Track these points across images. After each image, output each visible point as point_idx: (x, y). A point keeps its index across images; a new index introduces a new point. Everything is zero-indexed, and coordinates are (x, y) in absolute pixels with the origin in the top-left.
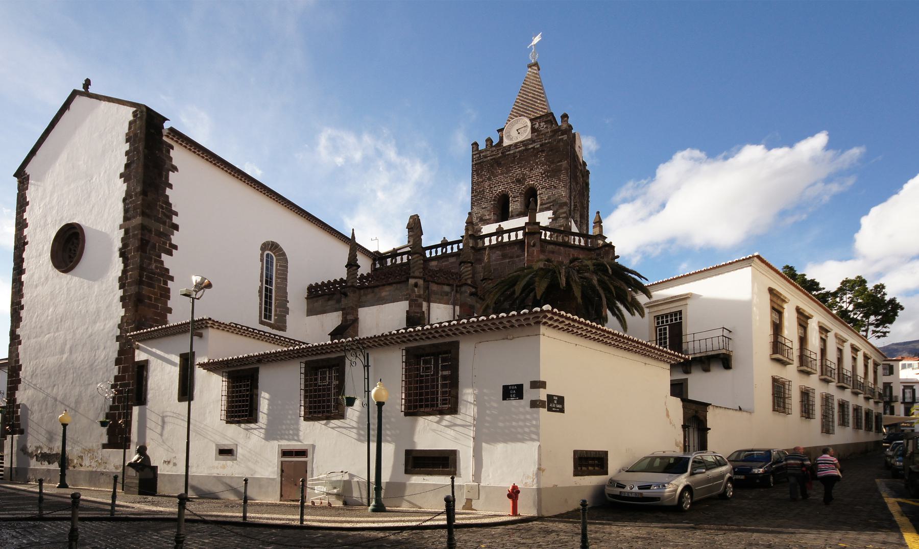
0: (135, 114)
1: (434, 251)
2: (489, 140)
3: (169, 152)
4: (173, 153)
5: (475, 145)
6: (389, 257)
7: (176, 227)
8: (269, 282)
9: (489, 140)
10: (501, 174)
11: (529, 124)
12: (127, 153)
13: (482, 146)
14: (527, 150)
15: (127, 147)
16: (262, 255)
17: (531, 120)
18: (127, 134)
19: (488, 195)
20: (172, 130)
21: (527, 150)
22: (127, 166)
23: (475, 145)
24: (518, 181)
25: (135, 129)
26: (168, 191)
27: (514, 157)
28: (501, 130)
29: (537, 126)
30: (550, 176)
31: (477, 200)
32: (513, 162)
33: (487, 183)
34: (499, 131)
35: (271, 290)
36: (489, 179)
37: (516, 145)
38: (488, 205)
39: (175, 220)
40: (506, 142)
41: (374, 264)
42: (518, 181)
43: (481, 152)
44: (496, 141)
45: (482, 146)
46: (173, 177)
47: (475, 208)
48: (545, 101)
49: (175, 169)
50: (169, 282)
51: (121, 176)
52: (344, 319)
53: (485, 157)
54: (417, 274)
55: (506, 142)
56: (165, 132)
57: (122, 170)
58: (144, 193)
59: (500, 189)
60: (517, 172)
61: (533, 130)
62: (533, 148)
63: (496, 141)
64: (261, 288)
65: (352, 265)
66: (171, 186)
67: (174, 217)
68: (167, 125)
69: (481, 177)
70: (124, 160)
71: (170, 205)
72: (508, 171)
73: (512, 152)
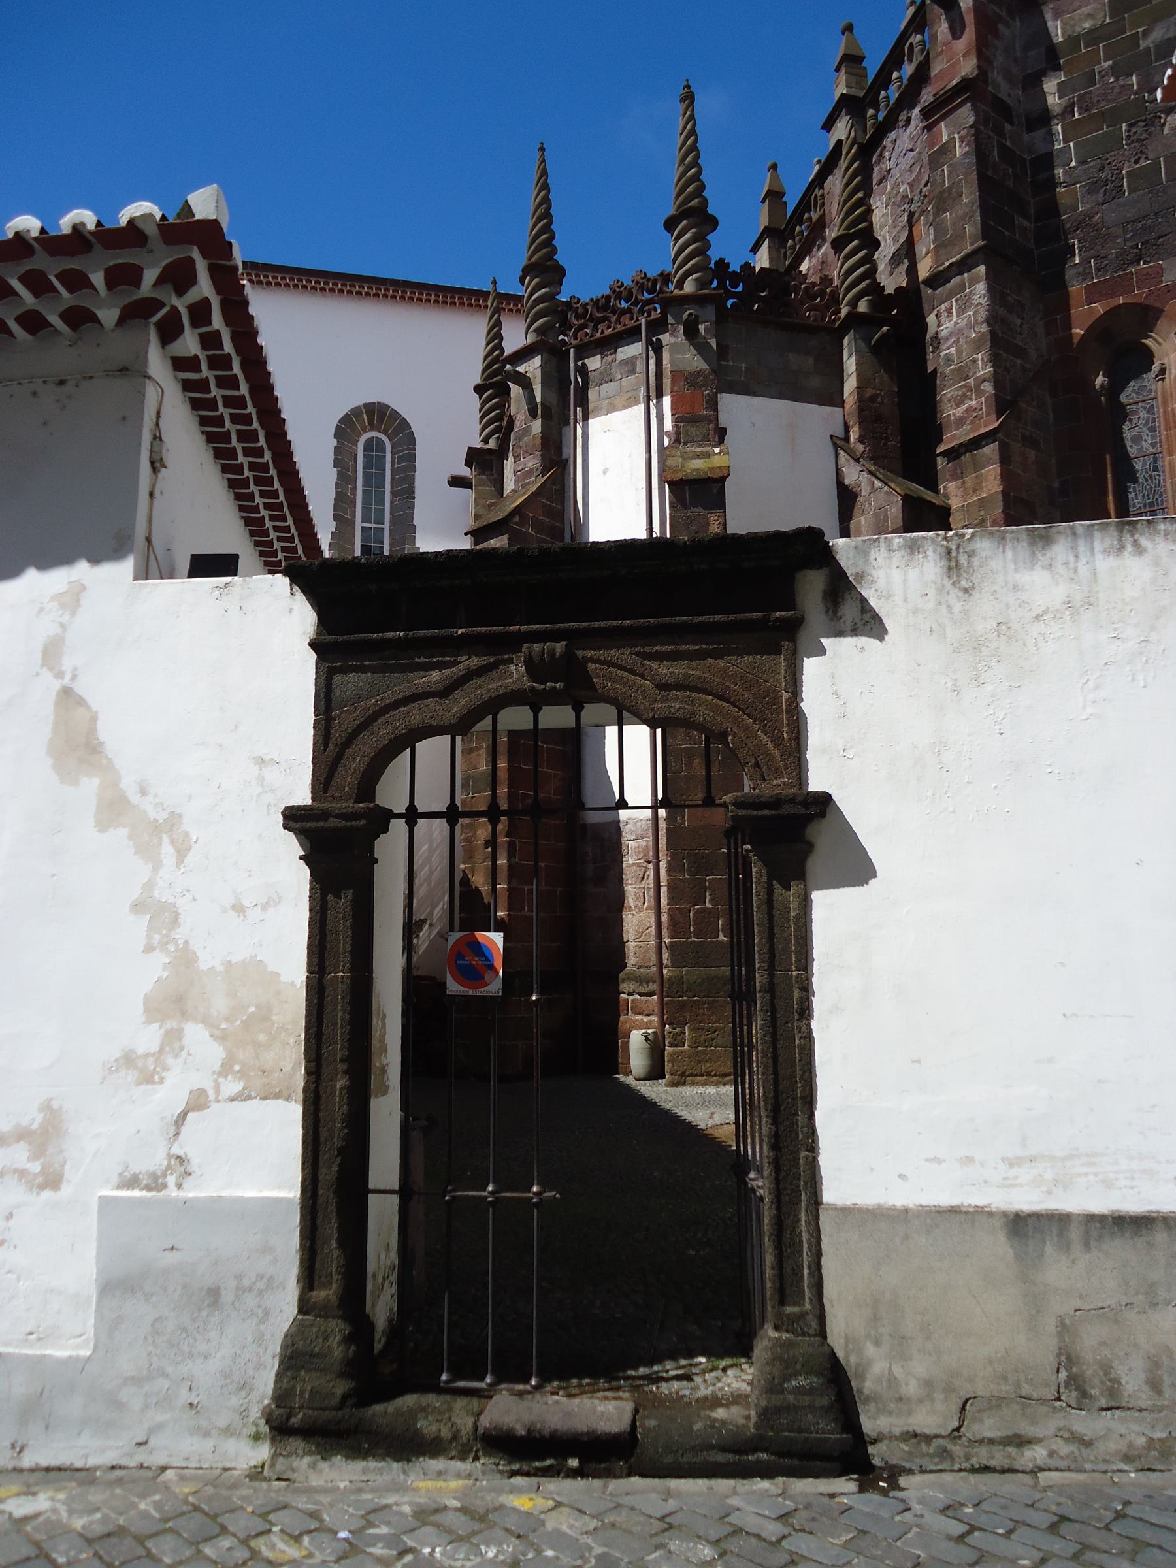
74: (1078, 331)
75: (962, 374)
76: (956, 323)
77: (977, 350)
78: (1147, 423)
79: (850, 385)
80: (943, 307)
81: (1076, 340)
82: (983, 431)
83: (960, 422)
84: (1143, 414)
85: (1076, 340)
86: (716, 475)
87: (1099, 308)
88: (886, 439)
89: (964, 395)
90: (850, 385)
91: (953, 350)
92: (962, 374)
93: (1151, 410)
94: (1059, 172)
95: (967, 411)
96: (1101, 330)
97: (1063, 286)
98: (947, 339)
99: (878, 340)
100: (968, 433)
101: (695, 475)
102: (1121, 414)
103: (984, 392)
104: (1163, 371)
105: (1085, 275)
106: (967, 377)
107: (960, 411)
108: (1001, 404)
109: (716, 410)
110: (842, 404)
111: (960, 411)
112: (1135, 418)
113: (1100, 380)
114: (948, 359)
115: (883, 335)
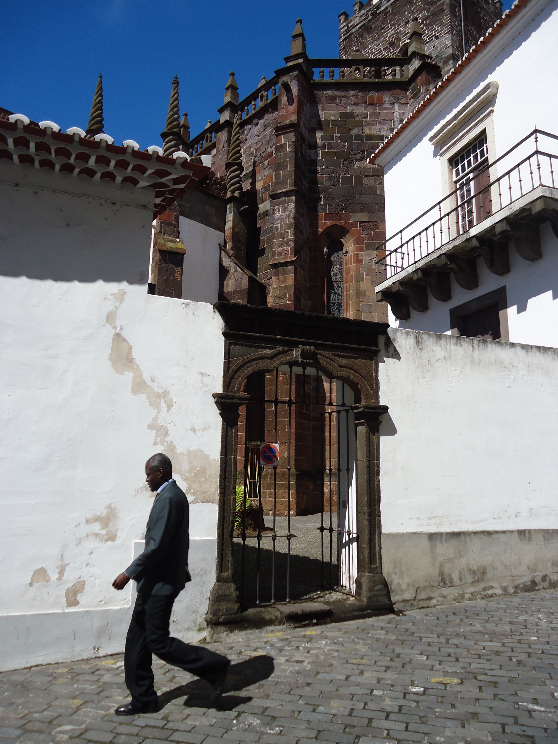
27: (386, 15)
30: (430, 24)
72: (380, 35)
73: (383, 8)
74: (321, 230)
75: (282, 236)
76: (281, 215)
77: (289, 228)
78: (339, 270)
79: (229, 225)
80: (276, 207)
81: (319, 233)
82: (289, 260)
83: (279, 254)
84: (338, 266)
85: (319, 233)
86: (181, 252)
87: (329, 224)
88: (241, 250)
89: (282, 244)
90: (229, 225)
91: (279, 225)
92: (282, 236)
93: (341, 265)
94: (319, 168)
95: (283, 250)
96: (328, 231)
97: (316, 211)
98: (277, 220)
99: (243, 210)
100: (282, 259)
101: (171, 250)
102: (330, 264)
103: (290, 245)
104: (347, 252)
105: (324, 210)
106: (284, 238)
107: (280, 250)
108: (297, 251)
109: (178, 222)
110: (224, 231)
111: (280, 250)
112: (335, 267)
113: (325, 250)
114: (277, 228)
115: (246, 209)
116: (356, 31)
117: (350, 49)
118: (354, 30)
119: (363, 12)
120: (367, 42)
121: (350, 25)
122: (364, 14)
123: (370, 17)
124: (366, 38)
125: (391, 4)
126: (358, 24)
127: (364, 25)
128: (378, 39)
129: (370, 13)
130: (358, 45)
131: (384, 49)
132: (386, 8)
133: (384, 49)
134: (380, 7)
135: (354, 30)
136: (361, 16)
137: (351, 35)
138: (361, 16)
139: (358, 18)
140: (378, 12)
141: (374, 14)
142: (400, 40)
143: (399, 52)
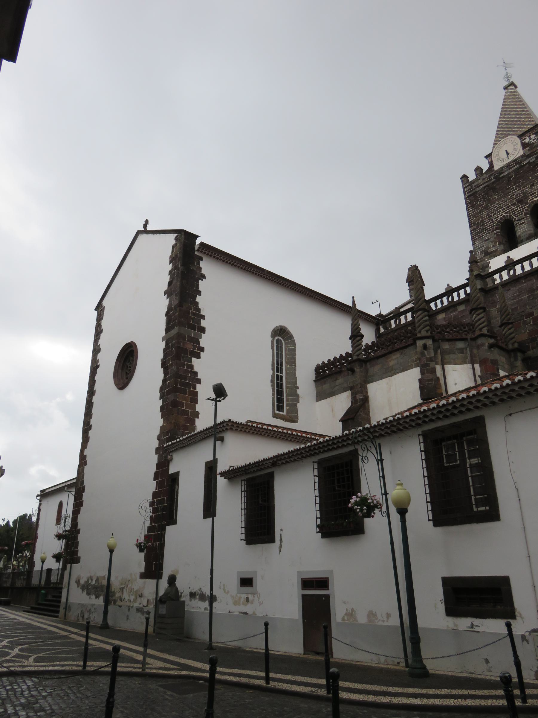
0: (176, 239)
1: (439, 302)
2: (478, 170)
3: (199, 264)
4: (202, 264)
5: (464, 178)
6: (391, 318)
7: (203, 330)
8: (279, 370)
9: (478, 170)
10: (500, 198)
11: (518, 141)
12: (170, 272)
13: (472, 177)
14: (522, 167)
15: (170, 267)
16: (272, 342)
17: (520, 137)
18: (170, 257)
19: (489, 225)
20: (202, 244)
21: (522, 167)
22: (170, 284)
23: (464, 178)
24: (520, 201)
25: (176, 251)
26: (198, 299)
27: (509, 178)
28: (488, 156)
29: (527, 140)
31: (477, 234)
32: (509, 183)
33: (485, 213)
34: (486, 157)
35: (282, 377)
36: (487, 208)
37: (508, 166)
38: (492, 236)
39: (203, 323)
40: (496, 167)
41: (378, 330)
42: (520, 201)
43: (473, 182)
44: (485, 167)
45: (472, 177)
46: (202, 285)
47: (476, 242)
48: (529, 114)
49: (203, 277)
50: (198, 385)
51: (166, 293)
52: (354, 401)
53: (478, 186)
54: (424, 333)
55: (496, 167)
56: (196, 248)
57: (166, 287)
58: (180, 305)
59: (500, 216)
60: (516, 192)
61: (524, 145)
62: (529, 163)
63: (485, 167)
64: (273, 377)
65: (356, 336)
66: (199, 293)
67: (202, 320)
68: (198, 241)
69: (477, 208)
70: (167, 279)
71: (199, 310)
72: (506, 195)
116: (481, 190)
117: (476, 203)
118: (478, 189)
119: (485, 176)
120: (493, 199)
121: (473, 185)
122: (486, 177)
123: (493, 180)
124: (492, 196)
125: (514, 171)
126: (481, 185)
127: (488, 186)
128: (505, 197)
129: (493, 177)
130: (484, 201)
131: (512, 205)
132: (508, 174)
133: (512, 205)
134: (503, 173)
135: (478, 189)
136: (484, 179)
137: (476, 192)
138: (484, 179)
139: (480, 182)
140: (500, 176)
141: (497, 178)
142: (527, 198)
143: (528, 207)
